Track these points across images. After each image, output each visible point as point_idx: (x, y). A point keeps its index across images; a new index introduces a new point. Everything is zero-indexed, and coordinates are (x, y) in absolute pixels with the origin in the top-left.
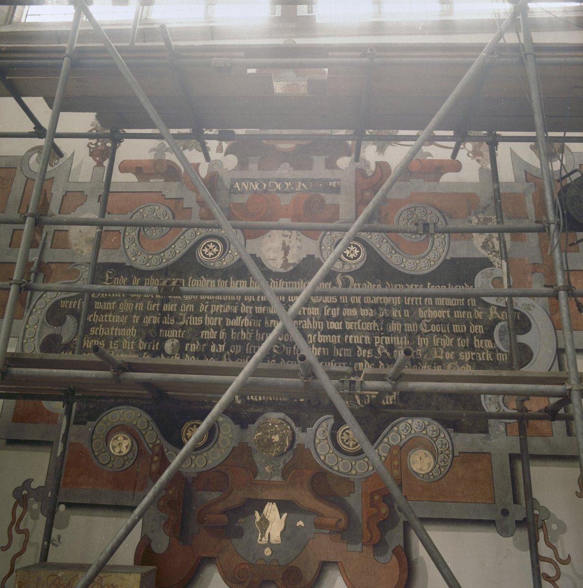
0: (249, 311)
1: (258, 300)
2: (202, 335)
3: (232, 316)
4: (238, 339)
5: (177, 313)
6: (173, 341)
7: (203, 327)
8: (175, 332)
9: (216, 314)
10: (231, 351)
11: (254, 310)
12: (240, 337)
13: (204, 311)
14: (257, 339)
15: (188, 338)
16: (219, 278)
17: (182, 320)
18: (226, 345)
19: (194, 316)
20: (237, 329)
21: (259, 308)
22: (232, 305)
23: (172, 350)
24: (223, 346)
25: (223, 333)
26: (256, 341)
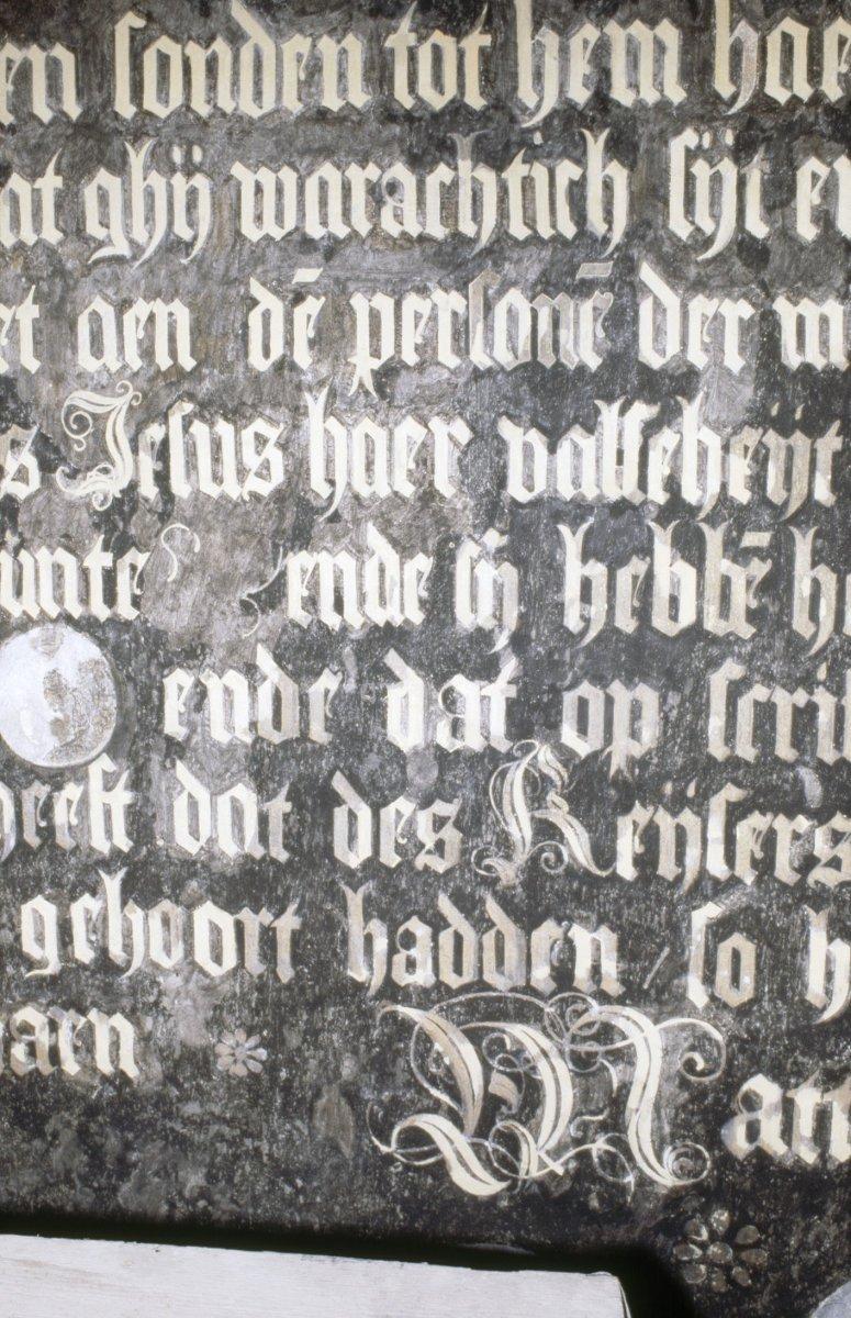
0: (715, 347)
1: (807, 231)
2: (296, 590)
3: (554, 397)
4: (626, 624)
5: (46, 387)
6: (50, 647)
7: (297, 518)
8: (58, 570)
9: (405, 385)
10: (568, 734)
11: (765, 338)
12: (643, 613)
13: (284, 365)
14: (800, 623)
15: (175, 620)
16: (396, 11)
17: (99, 455)
18: (528, 682)
19: (207, 409)
20: (617, 531)
21: (807, 308)
22: (547, 284)
23: (58, 726)
24: (500, 690)
25: (487, 572)
26: (796, 645)
